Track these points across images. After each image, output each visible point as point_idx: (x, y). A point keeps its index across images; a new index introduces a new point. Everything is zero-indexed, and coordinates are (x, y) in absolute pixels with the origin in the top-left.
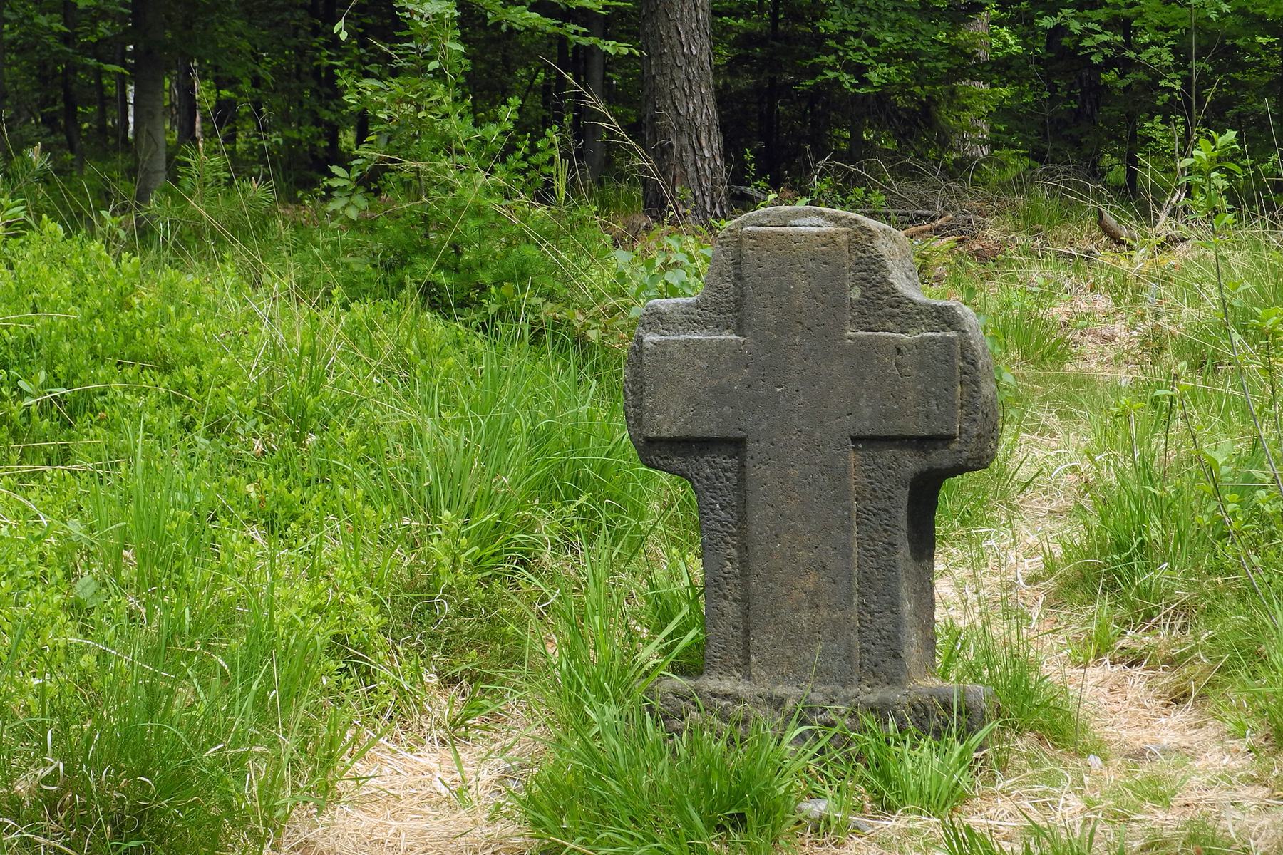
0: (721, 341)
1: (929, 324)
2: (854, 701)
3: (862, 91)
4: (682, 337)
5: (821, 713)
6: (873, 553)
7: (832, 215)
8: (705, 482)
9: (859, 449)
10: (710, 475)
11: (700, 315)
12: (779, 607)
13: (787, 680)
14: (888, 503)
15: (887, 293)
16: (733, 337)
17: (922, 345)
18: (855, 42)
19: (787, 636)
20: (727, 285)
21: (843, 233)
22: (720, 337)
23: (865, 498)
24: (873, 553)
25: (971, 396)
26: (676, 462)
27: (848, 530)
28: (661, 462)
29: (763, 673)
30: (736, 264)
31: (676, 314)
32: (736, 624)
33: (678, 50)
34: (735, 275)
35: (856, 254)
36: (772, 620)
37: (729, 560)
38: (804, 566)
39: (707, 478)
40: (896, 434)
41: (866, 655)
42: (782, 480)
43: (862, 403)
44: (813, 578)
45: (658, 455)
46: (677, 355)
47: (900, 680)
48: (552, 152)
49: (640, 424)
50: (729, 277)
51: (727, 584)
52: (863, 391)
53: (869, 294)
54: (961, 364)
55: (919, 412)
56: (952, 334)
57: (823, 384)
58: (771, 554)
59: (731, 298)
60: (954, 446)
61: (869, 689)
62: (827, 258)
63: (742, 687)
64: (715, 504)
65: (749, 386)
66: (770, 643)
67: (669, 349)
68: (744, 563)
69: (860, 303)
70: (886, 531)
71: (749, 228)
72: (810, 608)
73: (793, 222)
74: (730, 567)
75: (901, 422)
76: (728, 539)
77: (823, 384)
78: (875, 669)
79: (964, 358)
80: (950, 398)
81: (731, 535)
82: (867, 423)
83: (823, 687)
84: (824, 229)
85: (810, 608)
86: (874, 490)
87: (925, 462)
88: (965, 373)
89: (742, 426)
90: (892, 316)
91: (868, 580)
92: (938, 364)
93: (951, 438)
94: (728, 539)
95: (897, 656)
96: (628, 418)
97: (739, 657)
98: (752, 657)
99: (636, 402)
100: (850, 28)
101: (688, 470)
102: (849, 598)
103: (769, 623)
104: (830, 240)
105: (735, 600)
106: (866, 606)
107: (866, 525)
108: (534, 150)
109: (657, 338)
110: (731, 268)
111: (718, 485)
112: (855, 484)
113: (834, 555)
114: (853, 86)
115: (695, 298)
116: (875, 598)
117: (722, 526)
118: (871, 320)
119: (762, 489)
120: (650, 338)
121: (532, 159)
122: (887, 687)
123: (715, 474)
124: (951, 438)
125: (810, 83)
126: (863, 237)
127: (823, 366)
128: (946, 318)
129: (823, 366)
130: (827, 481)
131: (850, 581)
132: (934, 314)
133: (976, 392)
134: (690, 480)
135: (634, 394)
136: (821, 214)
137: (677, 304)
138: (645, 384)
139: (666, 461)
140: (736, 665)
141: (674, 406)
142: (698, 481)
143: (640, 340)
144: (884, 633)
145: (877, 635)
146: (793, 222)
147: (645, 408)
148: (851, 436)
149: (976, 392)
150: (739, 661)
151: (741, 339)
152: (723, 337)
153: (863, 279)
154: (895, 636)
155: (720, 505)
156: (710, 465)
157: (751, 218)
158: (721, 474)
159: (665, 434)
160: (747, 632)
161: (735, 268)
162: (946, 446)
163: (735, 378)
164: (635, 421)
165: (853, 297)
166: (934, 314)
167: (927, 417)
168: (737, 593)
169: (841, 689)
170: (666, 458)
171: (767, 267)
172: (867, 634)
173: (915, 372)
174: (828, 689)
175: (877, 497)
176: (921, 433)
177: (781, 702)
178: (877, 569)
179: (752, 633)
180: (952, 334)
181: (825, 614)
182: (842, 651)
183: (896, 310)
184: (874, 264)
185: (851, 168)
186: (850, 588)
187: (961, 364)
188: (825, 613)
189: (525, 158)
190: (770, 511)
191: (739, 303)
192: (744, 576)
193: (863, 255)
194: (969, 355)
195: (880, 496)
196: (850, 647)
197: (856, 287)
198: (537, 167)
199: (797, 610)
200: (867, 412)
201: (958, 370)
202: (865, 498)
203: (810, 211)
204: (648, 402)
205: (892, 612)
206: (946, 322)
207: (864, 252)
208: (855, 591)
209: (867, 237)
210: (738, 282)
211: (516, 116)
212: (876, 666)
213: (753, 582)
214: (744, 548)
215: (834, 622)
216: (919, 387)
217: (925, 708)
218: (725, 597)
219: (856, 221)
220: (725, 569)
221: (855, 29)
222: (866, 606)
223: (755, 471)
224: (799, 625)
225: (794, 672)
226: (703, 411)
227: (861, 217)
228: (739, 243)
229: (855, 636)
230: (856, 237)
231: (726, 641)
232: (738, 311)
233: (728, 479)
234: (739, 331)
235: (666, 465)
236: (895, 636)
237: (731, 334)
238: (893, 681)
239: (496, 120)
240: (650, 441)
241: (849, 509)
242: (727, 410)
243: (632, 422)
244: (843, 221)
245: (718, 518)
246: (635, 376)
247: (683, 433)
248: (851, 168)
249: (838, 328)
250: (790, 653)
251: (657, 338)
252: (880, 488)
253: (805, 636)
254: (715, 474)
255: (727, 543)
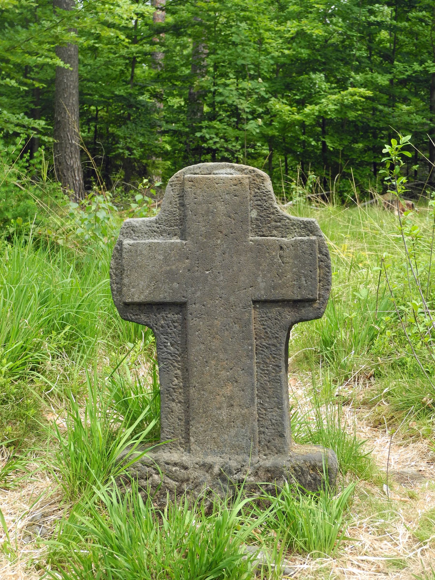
0: (172, 243)
1: (299, 232)
2: (256, 465)
3: (132, 157)
4: (147, 241)
5: (236, 474)
6: (266, 372)
7: (239, 167)
8: (161, 329)
9: (257, 308)
10: (164, 325)
11: (158, 228)
12: (208, 407)
13: (215, 453)
14: (275, 341)
15: (273, 213)
16: (179, 241)
17: (295, 245)
18: (129, 140)
19: (213, 425)
20: (175, 209)
21: (246, 178)
22: (171, 241)
23: (261, 338)
24: (266, 372)
25: (326, 275)
26: (143, 318)
27: (251, 358)
28: (133, 317)
29: (199, 449)
30: (180, 197)
31: (143, 227)
32: (181, 417)
33: (67, 141)
34: (180, 203)
35: (254, 191)
36: (204, 415)
37: (176, 377)
38: (223, 380)
39: (162, 327)
40: (280, 298)
41: (262, 436)
42: (210, 328)
43: (260, 280)
44: (230, 388)
45: (131, 313)
46: (144, 252)
47: (284, 451)
48: (41, 158)
49: (120, 295)
50: (176, 205)
51: (175, 392)
52: (260, 273)
53: (262, 214)
54: (319, 256)
55: (294, 284)
56: (313, 238)
57: (235, 268)
58: (203, 374)
59: (177, 217)
60: (316, 305)
61: (265, 457)
62: (237, 193)
63: (186, 458)
64: (167, 343)
65: (189, 270)
66: (202, 429)
67: (139, 248)
68: (186, 379)
69: (257, 219)
70: (274, 358)
71: (189, 175)
72: (228, 407)
73: (215, 172)
74: (176, 381)
75: (284, 292)
76: (175, 364)
77: (235, 268)
78: (269, 444)
79: (321, 252)
80: (313, 276)
81: (177, 362)
82: (263, 292)
83: (236, 456)
84: (234, 176)
85: (228, 407)
86: (266, 332)
87: (297, 315)
88: (322, 261)
89: (185, 295)
90: (276, 227)
91: (264, 388)
92: (306, 256)
93: (314, 300)
94: (175, 364)
95: (282, 436)
96: (112, 290)
97: (182, 438)
98: (191, 438)
99: (118, 281)
100: (127, 135)
101: (150, 322)
102: (252, 400)
103: (202, 417)
104: (240, 182)
105: (180, 402)
106: (263, 405)
107: (262, 354)
108: (32, 157)
109: (132, 242)
110: (177, 199)
111: (169, 331)
112: (255, 329)
113: (243, 374)
114: (129, 155)
115: (155, 218)
116: (268, 400)
117: (172, 356)
118: (264, 230)
119: (197, 333)
120: (127, 242)
121: (31, 161)
122: (276, 455)
123: (167, 324)
124: (314, 300)
125: (114, 153)
126: (258, 180)
127: (235, 258)
128: (309, 228)
129: (235, 258)
130: (238, 328)
131: (253, 389)
132: (302, 226)
133: (328, 272)
134: (151, 328)
135: (116, 275)
136: (233, 167)
137: (143, 221)
138: (124, 270)
139: (136, 317)
140: (181, 443)
141: (142, 283)
142: (157, 329)
143: (121, 243)
144: (274, 421)
145: (270, 422)
146: (215, 172)
147: (124, 285)
148: (252, 300)
149: (328, 272)
150: (182, 441)
151: (184, 242)
152: (172, 241)
153: (258, 205)
154: (281, 423)
155: (171, 343)
156: (164, 319)
157: (190, 170)
158: (171, 324)
159: (136, 300)
160: (187, 423)
161: (180, 200)
162: (311, 305)
163: (180, 266)
164: (117, 292)
165: (253, 216)
166: (302, 226)
167: (299, 288)
168: (181, 398)
169: (248, 458)
170: (137, 315)
171: (200, 198)
172: (263, 422)
173: (291, 261)
174: (240, 458)
175: (268, 337)
176: (295, 298)
177: (211, 467)
178: (269, 382)
179: (191, 423)
180: (313, 238)
181: (237, 411)
182: (248, 434)
183: (279, 224)
184: (265, 196)
185: (128, 184)
186: (253, 394)
187: (319, 256)
188: (237, 410)
189: (27, 161)
190: (202, 347)
191: (183, 220)
192: (186, 387)
193: (258, 191)
194: (324, 250)
195: (270, 336)
196: (253, 431)
197: (254, 210)
198: (33, 165)
199: (220, 408)
200: (262, 285)
201: (318, 259)
202: (261, 338)
203: (225, 165)
204: (126, 281)
205: (279, 408)
206: (309, 231)
207: (259, 189)
208: (255, 395)
209: (261, 180)
210: (181, 208)
211: (24, 142)
212: (269, 442)
213: (191, 391)
214: (186, 370)
215: (243, 416)
216: (294, 270)
217: (302, 469)
218: (173, 400)
219: (254, 171)
220: (174, 383)
221: (129, 136)
222: (263, 405)
223: (192, 322)
224: (221, 418)
225: (218, 447)
226: (160, 286)
227: (256, 169)
228: (183, 184)
229: (256, 424)
230: (254, 180)
231: (174, 428)
232: (182, 225)
233: (175, 327)
234: (183, 236)
235: (136, 319)
236: (281, 423)
237: (177, 239)
238: (280, 451)
239: (15, 144)
240: (127, 305)
241: (252, 345)
242: (176, 285)
243: (115, 293)
244: (245, 171)
245: (169, 351)
246: (117, 265)
247: (148, 299)
248: (128, 184)
249: (244, 234)
250: (215, 435)
251: (132, 242)
252: (270, 332)
253: (225, 424)
254: (167, 324)
255: (174, 367)
